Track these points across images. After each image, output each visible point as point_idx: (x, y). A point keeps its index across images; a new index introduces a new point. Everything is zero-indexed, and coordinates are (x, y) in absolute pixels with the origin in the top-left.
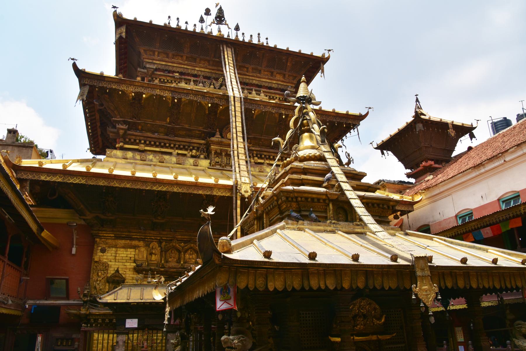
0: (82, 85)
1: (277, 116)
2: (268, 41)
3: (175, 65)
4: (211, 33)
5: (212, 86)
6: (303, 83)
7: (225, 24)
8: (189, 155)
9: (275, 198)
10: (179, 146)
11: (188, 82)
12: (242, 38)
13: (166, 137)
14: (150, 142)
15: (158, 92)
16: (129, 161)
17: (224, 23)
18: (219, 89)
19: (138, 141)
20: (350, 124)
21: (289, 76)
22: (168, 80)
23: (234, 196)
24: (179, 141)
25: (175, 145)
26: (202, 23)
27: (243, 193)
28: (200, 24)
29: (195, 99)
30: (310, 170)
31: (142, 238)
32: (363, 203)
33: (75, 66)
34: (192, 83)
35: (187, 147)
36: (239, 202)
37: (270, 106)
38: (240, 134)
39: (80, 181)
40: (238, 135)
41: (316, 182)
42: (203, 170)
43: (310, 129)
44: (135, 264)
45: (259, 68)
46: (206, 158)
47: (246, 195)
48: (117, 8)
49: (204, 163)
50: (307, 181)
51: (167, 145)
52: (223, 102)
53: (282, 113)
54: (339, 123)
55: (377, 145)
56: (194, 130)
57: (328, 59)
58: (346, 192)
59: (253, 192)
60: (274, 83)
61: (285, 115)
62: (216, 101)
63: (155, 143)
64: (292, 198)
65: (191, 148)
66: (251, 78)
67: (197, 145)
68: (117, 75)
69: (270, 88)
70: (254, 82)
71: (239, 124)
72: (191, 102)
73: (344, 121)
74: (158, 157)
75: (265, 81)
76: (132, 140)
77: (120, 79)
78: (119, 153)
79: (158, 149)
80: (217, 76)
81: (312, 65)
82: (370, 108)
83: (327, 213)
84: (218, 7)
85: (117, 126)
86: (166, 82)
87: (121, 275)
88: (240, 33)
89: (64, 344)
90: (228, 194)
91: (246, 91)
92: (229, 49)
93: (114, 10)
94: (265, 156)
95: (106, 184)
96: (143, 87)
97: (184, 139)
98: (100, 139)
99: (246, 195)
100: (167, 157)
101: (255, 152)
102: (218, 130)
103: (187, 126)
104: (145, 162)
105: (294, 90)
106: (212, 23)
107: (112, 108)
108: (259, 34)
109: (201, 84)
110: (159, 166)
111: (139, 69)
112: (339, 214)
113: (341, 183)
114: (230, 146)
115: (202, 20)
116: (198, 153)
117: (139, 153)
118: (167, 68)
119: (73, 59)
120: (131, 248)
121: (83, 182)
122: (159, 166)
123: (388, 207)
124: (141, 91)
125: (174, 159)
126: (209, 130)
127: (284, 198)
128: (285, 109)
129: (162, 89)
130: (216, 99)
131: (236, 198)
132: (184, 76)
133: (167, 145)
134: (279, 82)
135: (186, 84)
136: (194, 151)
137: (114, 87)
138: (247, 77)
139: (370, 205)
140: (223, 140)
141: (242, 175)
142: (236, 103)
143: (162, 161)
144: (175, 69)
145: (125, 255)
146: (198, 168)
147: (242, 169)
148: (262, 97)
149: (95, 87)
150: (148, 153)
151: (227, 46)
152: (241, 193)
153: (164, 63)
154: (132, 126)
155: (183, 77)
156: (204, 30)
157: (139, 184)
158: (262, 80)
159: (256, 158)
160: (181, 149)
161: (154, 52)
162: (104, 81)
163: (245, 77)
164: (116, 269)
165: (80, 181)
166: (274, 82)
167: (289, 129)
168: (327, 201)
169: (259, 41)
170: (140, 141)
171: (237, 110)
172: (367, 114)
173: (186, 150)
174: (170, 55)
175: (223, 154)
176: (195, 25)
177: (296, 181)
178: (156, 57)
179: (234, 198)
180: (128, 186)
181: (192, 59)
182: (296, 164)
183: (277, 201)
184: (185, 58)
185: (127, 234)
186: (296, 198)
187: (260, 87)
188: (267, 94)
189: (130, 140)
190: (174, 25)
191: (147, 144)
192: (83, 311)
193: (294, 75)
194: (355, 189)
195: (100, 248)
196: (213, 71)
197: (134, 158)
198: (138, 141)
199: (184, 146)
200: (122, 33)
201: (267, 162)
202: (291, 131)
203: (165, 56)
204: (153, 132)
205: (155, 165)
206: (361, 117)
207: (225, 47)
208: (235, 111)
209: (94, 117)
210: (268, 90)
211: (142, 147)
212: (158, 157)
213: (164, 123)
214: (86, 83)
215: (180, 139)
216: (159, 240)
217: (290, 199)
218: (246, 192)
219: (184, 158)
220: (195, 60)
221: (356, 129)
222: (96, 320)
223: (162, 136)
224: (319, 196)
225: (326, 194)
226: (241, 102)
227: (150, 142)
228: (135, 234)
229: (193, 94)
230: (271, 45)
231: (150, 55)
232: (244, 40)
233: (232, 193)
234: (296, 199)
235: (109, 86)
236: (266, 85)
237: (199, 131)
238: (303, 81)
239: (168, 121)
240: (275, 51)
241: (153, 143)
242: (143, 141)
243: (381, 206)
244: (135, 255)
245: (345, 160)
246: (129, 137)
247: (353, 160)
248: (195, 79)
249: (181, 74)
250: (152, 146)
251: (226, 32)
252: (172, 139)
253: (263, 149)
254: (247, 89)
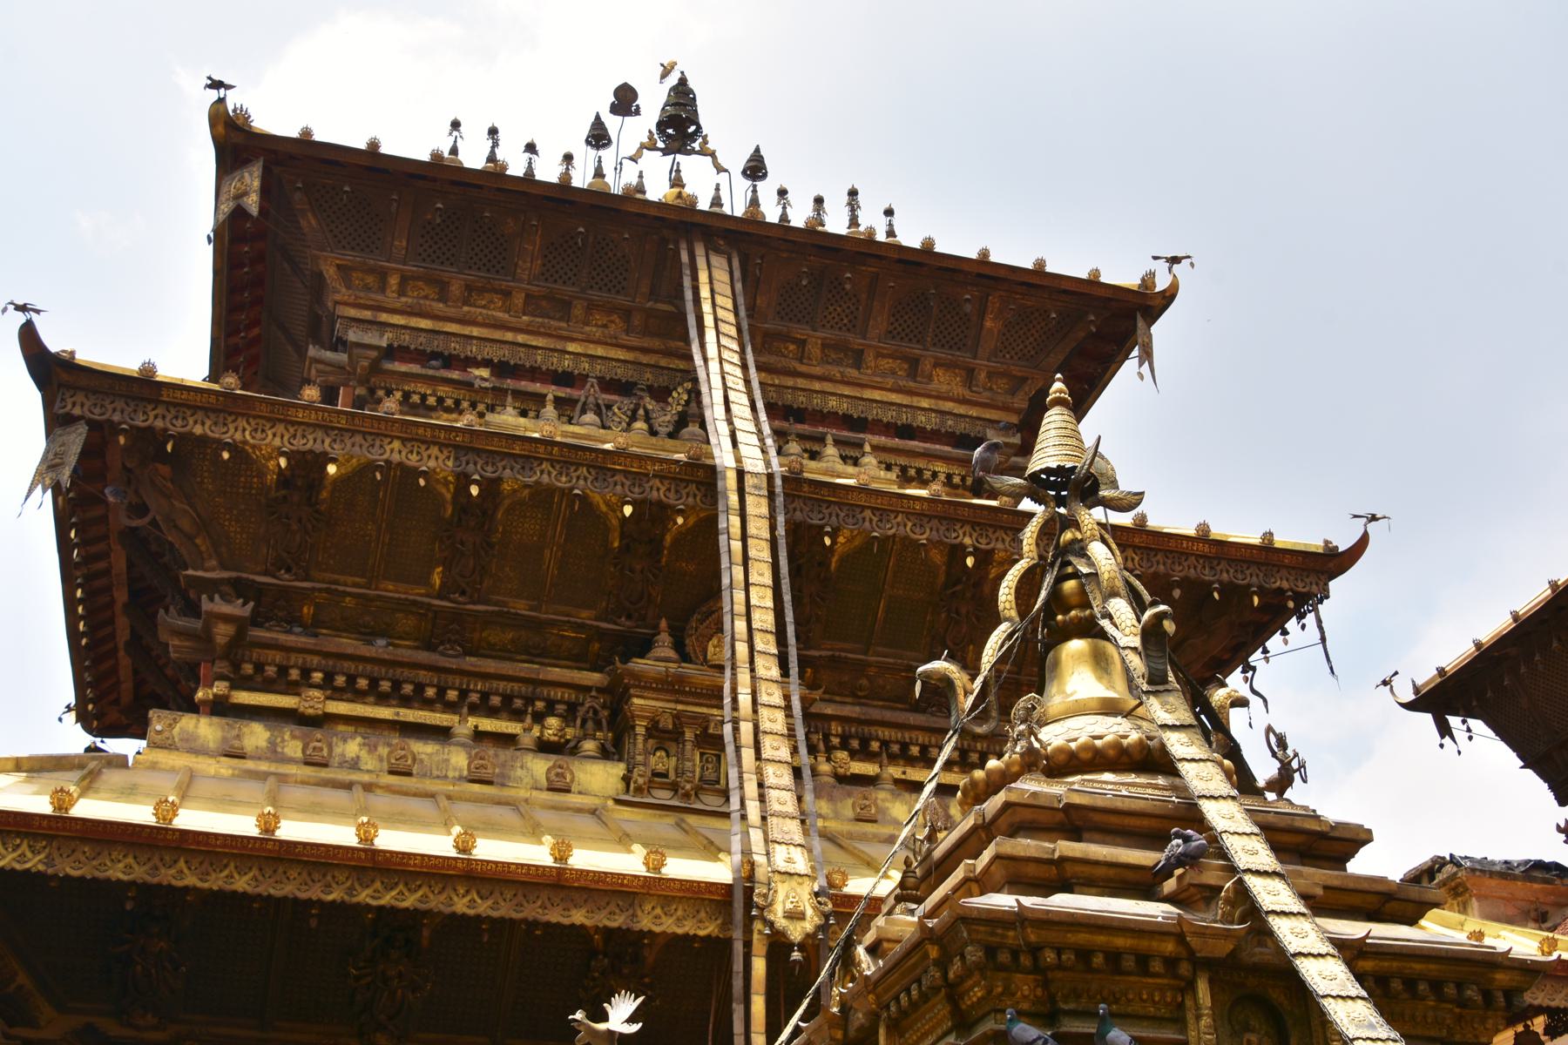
0: (55, 421)
1: (937, 557)
2: (896, 220)
3: (475, 332)
4: (640, 189)
5: (640, 425)
6: (1056, 410)
7: (703, 152)
8: (527, 740)
9: (934, 952)
10: (485, 696)
11: (530, 405)
12: (779, 210)
13: (423, 656)
14: (352, 679)
15: (394, 452)
16: (249, 765)
17: (696, 146)
18: (671, 436)
19: (294, 674)
20: (1280, 591)
21: (990, 375)
22: (440, 400)
23: (737, 934)
24: (485, 676)
25: (464, 694)
26: (598, 147)
27: (781, 923)
28: (592, 152)
29: (563, 482)
30: (1097, 817)
32: (1360, 978)
33: (29, 337)
34: (549, 410)
35: (518, 703)
36: (759, 966)
37: (907, 514)
38: (767, 644)
39: (22, 858)
40: (759, 645)
41: (1130, 875)
42: (593, 812)
43: (1093, 618)
45: (856, 341)
46: (606, 754)
47: (796, 932)
48: (231, 87)
49: (599, 777)
50: (1087, 870)
51: (430, 692)
52: (688, 498)
53: (963, 547)
54: (1228, 589)
55: (1417, 690)
56: (553, 623)
57: (1169, 296)
58: (1277, 924)
59: (826, 916)
60: (923, 410)
61: (976, 552)
62: (658, 492)
63: (374, 683)
64: (1015, 954)
65: (540, 705)
66: (817, 386)
67: (568, 695)
68: (214, 376)
69: (907, 432)
70: (833, 403)
71: (762, 598)
72: (543, 496)
73: (1252, 578)
74: (383, 751)
75: (882, 399)
76: (271, 671)
77: (228, 396)
78: (206, 729)
79: (385, 713)
80: (663, 381)
81: (1096, 328)
82: (1374, 518)
83: (1183, 1029)
84: (673, 80)
85: (206, 605)
86: (432, 409)
88: (767, 191)
90: (709, 929)
91: (794, 447)
92: (718, 261)
93: (213, 95)
94: (885, 744)
95: (140, 873)
96: (327, 429)
97: (507, 668)
98: (125, 661)
99: (796, 932)
100: (424, 749)
101: (836, 728)
102: (663, 624)
103: (521, 607)
104: (324, 774)
105: (1016, 440)
106: (643, 146)
107: (185, 524)
108: (853, 193)
109: (590, 417)
110: (389, 789)
111: (313, 351)
112: (1247, 1028)
113: (1251, 881)
114: (722, 698)
115: (598, 137)
116: (570, 732)
117: (298, 730)
118: (437, 344)
119: (23, 308)
121: (34, 863)
122: (389, 789)
123: (1487, 995)
124: (318, 448)
125: (459, 760)
126: (624, 624)
127: (973, 954)
128: (974, 525)
129: (411, 436)
130: (657, 482)
131: (748, 944)
132: (516, 379)
133: (430, 692)
134: (948, 406)
135: (524, 414)
136: (553, 722)
137: (198, 430)
138: (801, 383)
139: (1396, 985)
140: (689, 669)
141: (775, 834)
142: (749, 500)
143: (401, 765)
144: (473, 350)
146: (573, 799)
147: (776, 807)
148: (870, 473)
149: (114, 429)
150: (341, 728)
151: (711, 248)
152: (771, 924)
153: (425, 324)
154: (272, 607)
155: (510, 383)
156: (610, 178)
157: (293, 874)
158: (868, 394)
159: (842, 755)
160: (492, 713)
161: (383, 276)
162: (157, 402)
163: (790, 382)
165: (22, 858)
166: (925, 403)
167: (997, 620)
168: (1184, 969)
169: (854, 222)
170: (306, 673)
171: (751, 530)
172: (1362, 543)
173: (517, 715)
174: (455, 289)
175: (689, 735)
176: (568, 158)
177: (1031, 870)
178: (391, 298)
179: (738, 947)
180: (242, 884)
181: (552, 307)
182: (1031, 786)
183: (943, 964)
184: (519, 300)
186: (1035, 950)
187: (860, 424)
188: (892, 459)
189: (259, 667)
190: (473, 157)
191: (336, 689)
193: (1016, 371)
194: (1319, 905)
196: (645, 359)
197: (273, 753)
198: (294, 674)
199: (507, 699)
200: (245, 194)
201: (895, 771)
202: (1003, 629)
203: (427, 291)
204: (368, 635)
205: (368, 788)
206: (1334, 562)
207: (700, 251)
208: (744, 538)
209: (102, 565)
210: (897, 442)
211: (313, 701)
212: (383, 751)
213: (416, 593)
214: (77, 411)
215: (490, 666)
217: (1004, 957)
218: (795, 916)
219: (505, 754)
220: (563, 308)
221: (1310, 619)
223: (406, 654)
224: (1144, 944)
225: (1176, 932)
226: (771, 496)
227: (352, 679)
229: (552, 462)
230: (910, 238)
231: (367, 288)
232: (784, 217)
233: (727, 923)
234: (1035, 960)
235: (177, 428)
236: (888, 416)
237: (579, 627)
238: (1059, 402)
239: (437, 580)
240: (926, 265)
241: (363, 683)
242: (317, 676)
243: (1450, 990)
245: (1264, 769)
246: (256, 654)
247: (1302, 766)
248: (563, 392)
249: (501, 369)
250: (359, 696)
251: (704, 183)
252: (452, 663)
253: (876, 714)
254: (802, 437)
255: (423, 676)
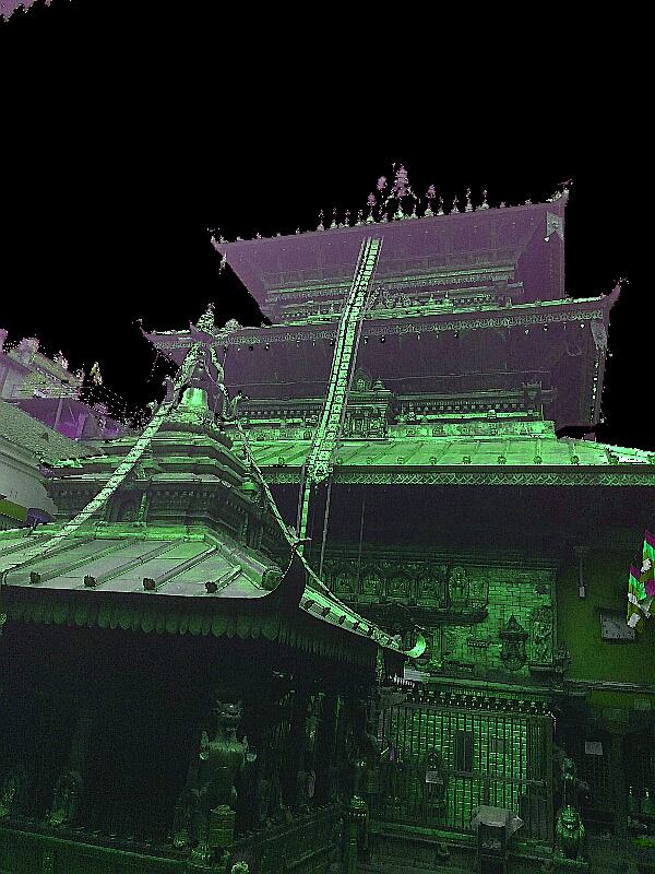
36: (308, 492)
60: (472, 275)
75: (455, 276)
79: (267, 421)
99: (317, 479)
215: (301, 401)
250: (260, 417)
255: (277, 408)
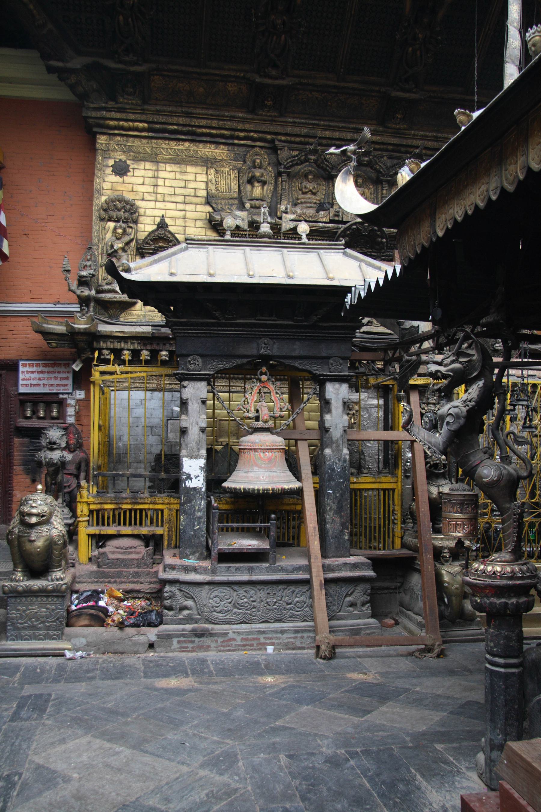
31: (222, 136)
44: (209, 209)
87: (173, 235)
89: (42, 414)
120: (196, 164)
145: (182, 184)
164: (158, 220)
185: (181, 120)
192: (81, 325)
195: (111, 162)
216: (272, 141)
222: (117, 353)
228: (204, 122)
244: (207, 183)
